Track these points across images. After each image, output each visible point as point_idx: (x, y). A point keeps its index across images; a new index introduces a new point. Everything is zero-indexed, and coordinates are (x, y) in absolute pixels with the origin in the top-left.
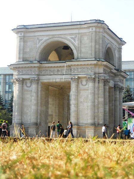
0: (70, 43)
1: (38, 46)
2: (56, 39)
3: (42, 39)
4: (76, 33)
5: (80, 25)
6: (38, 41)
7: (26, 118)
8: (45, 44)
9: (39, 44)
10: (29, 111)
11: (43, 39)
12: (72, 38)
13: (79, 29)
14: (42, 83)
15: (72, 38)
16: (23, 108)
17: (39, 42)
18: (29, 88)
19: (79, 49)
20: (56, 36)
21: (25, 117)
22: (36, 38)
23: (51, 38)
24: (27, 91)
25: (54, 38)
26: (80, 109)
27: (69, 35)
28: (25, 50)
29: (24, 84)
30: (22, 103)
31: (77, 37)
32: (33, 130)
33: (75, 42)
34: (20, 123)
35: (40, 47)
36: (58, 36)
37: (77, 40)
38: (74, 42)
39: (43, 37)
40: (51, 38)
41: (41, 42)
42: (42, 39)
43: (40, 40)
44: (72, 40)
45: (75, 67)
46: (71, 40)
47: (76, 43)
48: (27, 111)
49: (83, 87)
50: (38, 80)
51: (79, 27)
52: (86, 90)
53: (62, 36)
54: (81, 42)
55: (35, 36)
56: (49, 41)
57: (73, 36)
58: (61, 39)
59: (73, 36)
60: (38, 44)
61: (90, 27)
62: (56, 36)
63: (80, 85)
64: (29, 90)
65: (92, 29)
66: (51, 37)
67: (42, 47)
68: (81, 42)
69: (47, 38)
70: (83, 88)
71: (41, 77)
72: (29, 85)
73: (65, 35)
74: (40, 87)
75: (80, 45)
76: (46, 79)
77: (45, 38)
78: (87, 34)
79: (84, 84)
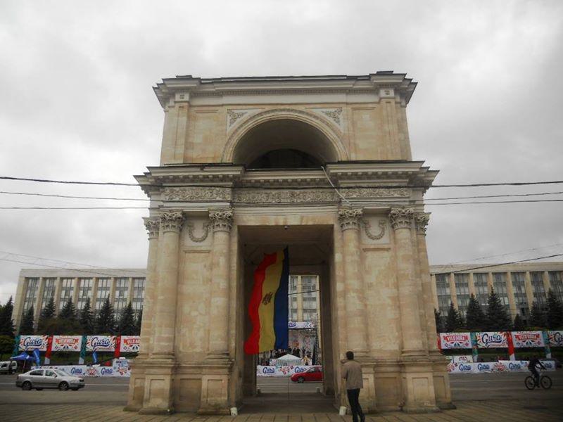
0: (324, 125)
2: (283, 113)
3: (243, 114)
4: (339, 103)
5: (353, 82)
6: (229, 118)
7: (187, 334)
8: (250, 125)
9: (233, 125)
10: (200, 314)
11: (246, 113)
13: (347, 94)
16: (179, 303)
18: (198, 244)
19: (352, 141)
20: (282, 107)
21: (184, 330)
23: (268, 112)
24: (195, 252)
25: (276, 110)
26: (369, 307)
27: (318, 106)
28: (190, 140)
29: (186, 231)
30: (177, 290)
31: (344, 112)
33: (338, 122)
34: (169, 354)
35: (236, 130)
36: (287, 107)
37: (344, 119)
38: (336, 124)
39: (244, 107)
40: (268, 112)
41: (238, 120)
42: (243, 114)
44: (331, 120)
46: (326, 117)
47: (342, 126)
50: (231, 220)
51: (351, 86)
54: (354, 124)
55: (223, 105)
56: (261, 119)
57: (333, 110)
58: (297, 114)
59: (333, 110)
60: (231, 123)
62: (282, 107)
63: (364, 236)
64: (199, 249)
66: (267, 108)
67: (242, 132)
68: (354, 124)
69: (259, 111)
70: (374, 244)
71: (240, 211)
72: (199, 233)
73: (307, 106)
74: (235, 239)
75: (354, 131)
76: (252, 217)
77: (251, 112)
78: (370, 106)
79: (376, 235)
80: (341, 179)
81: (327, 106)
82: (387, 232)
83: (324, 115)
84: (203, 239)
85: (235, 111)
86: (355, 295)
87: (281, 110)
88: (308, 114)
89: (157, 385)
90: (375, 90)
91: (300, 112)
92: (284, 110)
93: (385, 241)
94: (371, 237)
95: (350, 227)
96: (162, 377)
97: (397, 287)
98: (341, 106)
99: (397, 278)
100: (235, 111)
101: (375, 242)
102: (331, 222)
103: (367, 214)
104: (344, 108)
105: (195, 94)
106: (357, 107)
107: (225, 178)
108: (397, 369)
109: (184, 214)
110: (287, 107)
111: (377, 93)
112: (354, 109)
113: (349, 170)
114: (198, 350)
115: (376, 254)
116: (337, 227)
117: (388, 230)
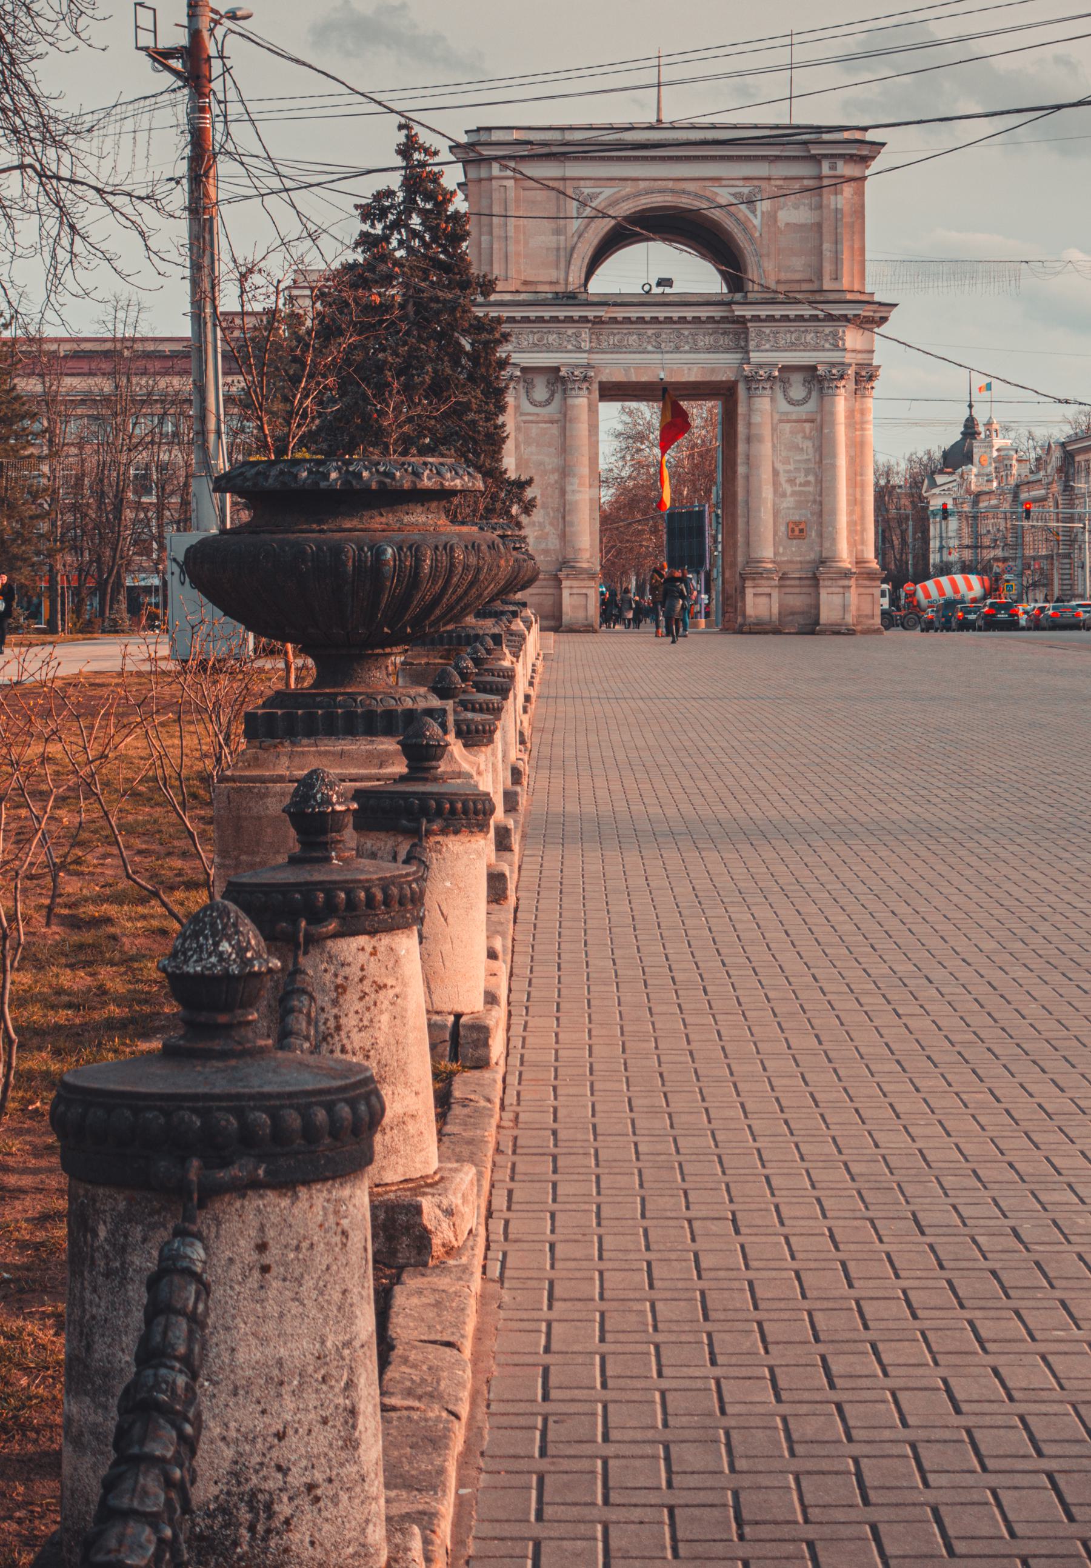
13: (771, 161)
38: (751, 216)
49: (791, 408)
57: (746, 190)
61: (825, 156)
65: (833, 167)
80: (750, 321)
82: (814, 394)
90: (817, 159)
93: (811, 406)
101: (797, 408)
103: (785, 369)
107: (584, 319)
109: (524, 370)
111: (819, 162)
113: (763, 312)
116: (741, 389)
117: (814, 394)
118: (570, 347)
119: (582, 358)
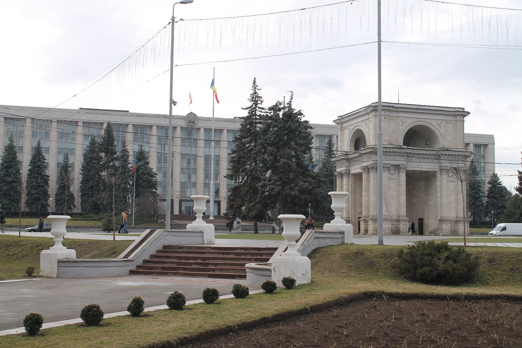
1: (401, 129)
5: (449, 112)
9: (403, 127)
12: (437, 124)
14: (407, 171)
15: (437, 124)
17: (403, 124)
18: (392, 176)
20: (421, 120)
22: (400, 120)
32: (405, 223)
36: (423, 120)
38: (440, 129)
39: (407, 118)
41: (405, 124)
42: (406, 122)
43: (403, 123)
44: (438, 127)
45: (446, 157)
46: (437, 126)
47: (442, 130)
48: (392, 202)
52: (453, 181)
53: (428, 121)
54: (446, 129)
55: (399, 117)
57: (439, 123)
59: (439, 123)
60: (402, 126)
61: (458, 115)
66: (416, 120)
68: (446, 129)
69: (412, 121)
77: (410, 121)
78: (453, 122)
79: (451, 176)
81: (437, 120)
83: (436, 124)
84: (394, 174)
85: (404, 120)
86: (445, 198)
87: (421, 121)
88: (430, 124)
89: (387, 226)
90: (456, 116)
91: (428, 123)
92: (421, 121)
94: (450, 177)
95: (445, 173)
96: (388, 223)
97: (457, 195)
98: (442, 121)
99: (457, 192)
100: (404, 120)
102: (437, 170)
104: (444, 122)
105: (389, 111)
106: (448, 122)
108: (455, 223)
110: (423, 120)
112: (447, 122)
114: (394, 215)
115: (450, 182)
118: (402, 160)
119: (405, 163)
